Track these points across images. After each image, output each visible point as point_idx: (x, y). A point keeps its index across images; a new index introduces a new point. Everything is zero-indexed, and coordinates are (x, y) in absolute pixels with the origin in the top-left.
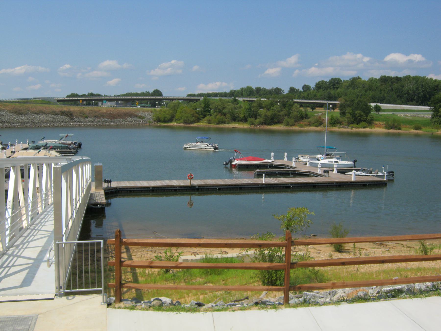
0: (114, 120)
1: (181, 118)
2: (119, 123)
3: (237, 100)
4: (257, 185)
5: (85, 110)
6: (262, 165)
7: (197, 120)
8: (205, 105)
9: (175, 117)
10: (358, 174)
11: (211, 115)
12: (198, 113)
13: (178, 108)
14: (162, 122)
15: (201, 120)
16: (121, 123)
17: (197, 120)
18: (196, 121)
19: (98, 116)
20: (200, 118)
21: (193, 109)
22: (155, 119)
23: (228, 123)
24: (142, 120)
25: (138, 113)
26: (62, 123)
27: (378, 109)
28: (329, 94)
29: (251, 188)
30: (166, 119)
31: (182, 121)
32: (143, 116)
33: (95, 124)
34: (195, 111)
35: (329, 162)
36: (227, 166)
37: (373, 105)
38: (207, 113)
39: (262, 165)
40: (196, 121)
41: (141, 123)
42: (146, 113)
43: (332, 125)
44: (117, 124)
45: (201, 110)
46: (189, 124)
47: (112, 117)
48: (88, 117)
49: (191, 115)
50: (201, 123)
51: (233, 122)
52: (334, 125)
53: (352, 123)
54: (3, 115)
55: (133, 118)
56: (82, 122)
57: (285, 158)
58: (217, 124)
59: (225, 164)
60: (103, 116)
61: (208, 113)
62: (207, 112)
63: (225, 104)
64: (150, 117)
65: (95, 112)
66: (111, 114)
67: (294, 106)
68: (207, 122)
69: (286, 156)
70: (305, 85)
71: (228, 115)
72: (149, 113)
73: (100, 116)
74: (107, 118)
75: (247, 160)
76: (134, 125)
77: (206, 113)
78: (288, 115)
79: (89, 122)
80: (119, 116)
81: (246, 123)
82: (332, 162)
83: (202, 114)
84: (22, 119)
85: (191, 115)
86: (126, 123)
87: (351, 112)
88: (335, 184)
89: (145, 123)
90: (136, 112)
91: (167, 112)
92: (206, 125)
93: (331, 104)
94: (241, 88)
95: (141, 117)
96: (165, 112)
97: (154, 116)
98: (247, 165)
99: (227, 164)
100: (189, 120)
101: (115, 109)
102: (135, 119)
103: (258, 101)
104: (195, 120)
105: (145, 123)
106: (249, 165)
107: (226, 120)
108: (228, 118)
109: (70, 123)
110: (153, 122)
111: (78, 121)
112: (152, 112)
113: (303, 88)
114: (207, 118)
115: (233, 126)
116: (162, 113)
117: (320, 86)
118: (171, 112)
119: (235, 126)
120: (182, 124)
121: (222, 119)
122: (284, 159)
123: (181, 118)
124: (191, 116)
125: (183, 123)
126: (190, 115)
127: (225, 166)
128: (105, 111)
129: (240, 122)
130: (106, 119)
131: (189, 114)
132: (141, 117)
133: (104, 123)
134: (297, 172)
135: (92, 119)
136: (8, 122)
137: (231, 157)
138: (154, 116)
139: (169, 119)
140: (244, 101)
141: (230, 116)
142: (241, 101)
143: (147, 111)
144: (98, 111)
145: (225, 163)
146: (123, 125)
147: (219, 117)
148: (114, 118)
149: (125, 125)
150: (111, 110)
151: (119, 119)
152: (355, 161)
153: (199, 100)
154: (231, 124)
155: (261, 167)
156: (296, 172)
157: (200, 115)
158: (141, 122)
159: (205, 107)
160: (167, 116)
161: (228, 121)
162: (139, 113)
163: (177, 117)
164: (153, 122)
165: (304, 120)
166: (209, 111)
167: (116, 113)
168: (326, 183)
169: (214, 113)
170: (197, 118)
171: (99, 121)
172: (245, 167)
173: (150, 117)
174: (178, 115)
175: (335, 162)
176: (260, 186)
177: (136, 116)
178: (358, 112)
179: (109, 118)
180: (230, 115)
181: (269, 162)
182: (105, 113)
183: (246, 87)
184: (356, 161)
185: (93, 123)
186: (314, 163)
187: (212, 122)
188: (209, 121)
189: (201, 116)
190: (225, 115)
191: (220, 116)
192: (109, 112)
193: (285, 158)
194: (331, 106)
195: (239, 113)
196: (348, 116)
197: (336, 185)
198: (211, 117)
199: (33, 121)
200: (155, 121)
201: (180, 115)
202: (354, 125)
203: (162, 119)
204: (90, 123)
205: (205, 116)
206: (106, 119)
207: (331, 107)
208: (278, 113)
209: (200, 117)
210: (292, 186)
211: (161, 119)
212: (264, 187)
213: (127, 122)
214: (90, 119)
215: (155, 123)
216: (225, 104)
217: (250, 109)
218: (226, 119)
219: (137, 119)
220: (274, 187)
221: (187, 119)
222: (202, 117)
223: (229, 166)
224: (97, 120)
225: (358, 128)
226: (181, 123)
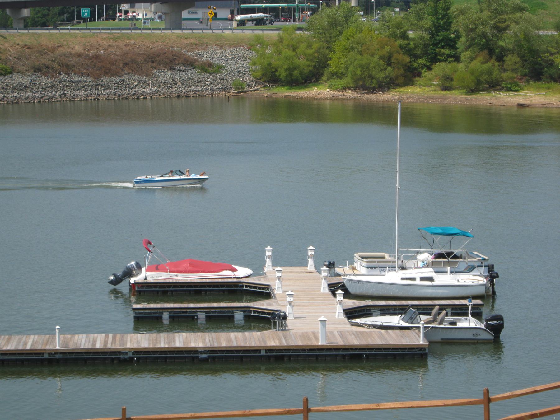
0: (106, 80)
1: (347, 68)
2: (125, 92)
4: (40, 354)
5: (6, 45)
6: (210, 286)
7: (404, 76)
8: (438, 19)
10: (380, 324)
11: (457, 59)
12: (409, 52)
14: (283, 86)
15: (419, 75)
16: (132, 92)
17: (404, 76)
18: (401, 80)
19: (48, 67)
20: (416, 69)
22: (259, 74)
23: (509, 90)
24: (209, 78)
25: (203, 52)
29: (22, 361)
30: (296, 73)
31: (347, 80)
32: (218, 61)
33: (34, 98)
34: (399, 42)
35: (403, 279)
36: (118, 287)
38: (443, 50)
39: (210, 286)
40: (401, 80)
41: (206, 90)
42: (229, 52)
44: (115, 94)
46: (372, 90)
47: (100, 68)
48: (11, 73)
49: (381, 58)
50: (418, 89)
51: (532, 83)
55: (180, 70)
57: (311, 262)
58: (473, 91)
59: (111, 282)
60: (68, 68)
61: (447, 52)
62: (442, 47)
63: (504, 16)
64: (242, 65)
65: (43, 51)
66: (97, 57)
68: (438, 85)
69: (312, 257)
71: (511, 60)
72: (242, 50)
73: (56, 65)
74: (82, 75)
75: (170, 272)
76: (178, 96)
77: (437, 50)
79: (15, 88)
80: (126, 64)
82: (413, 279)
83: (425, 54)
85: (381, 58)
86: (148, 90)
88: (263, 353)
89: (221, 89)
90: (193, 50)
92: (432, 94)
95: (207, 68)
96: (294, 50)
97: (254, 64)
98: (164, 287)
99: (117, 281)
100: (371, 77)
101: (115, 40)
102: (186, 76)
104: (397, 77)
105: (221, 89)
106: (169, 287)
107: (504, 75)
108: (514, 71)
110: (249, 85)
112: (251, 47)
114: (440, 68)
115: (522, 101)
116: (289, 53)
118: (315, 46)
119: (528, 102)
120: (350, 94)
121: (490, 72)
122: (306, 265)
123: (347, 68)
124: (382, 62)
125: (355, 89)
126: (376, 58)
127: (112, 287)
128: (78, 49)
129: (552, 84)
130: (76, 79)
131: (373, 55)
132: (210, 65)
133: (69, 93)
134: (254, 312)
135: (26, 80)
137: (131, 262)
138: (254, 64)
139: (306, 71)
141: (518, 60)
143: (236, 44)
144: (53, 50)
145: (112, 278)
146: (138, 98)
147: (479, 64)
148: (108, 72)
149: (145, 98)
150: (105, 43)
151: (126, 77)
152: (492, 275)
154: (522, 89)
155: (206, 291)
156: (250, 311)
157: (416, 57)
158: (205, 85)
159: (437, 28)
160: (302, 62)
161: (509, 81)
162: (203, 52)
163: (332, 68)
164: (249, 85)
166: (451, 44)
167: (118, 53)
168: (238, 351)
169: (467, 49)
170: (402, 71)
171: (52, 87)
172: (158, 291)
173: (242, 65)
176: (46, 356)
177: (191, 63)
179: (88, 75)
180: (522, 57)
181: (238, 278)
182: (79, 55)
184: (497, 276)
185: (29, 94)
186: (363, 282)
187: (454, 83)
188: (449, 78)
189: (422, 61)
190: (500, 59)
191: (483, 63)
192: (91, 53)
193: (311, 262)
195: (553, 51)
197: (269, 357)
200: (258, 80)
201: (342, 61)
203: (282, 74)
204: (16, 94)
206: (76, 79)
209: (416, 65)
210: (138, 359)
211: (277, 73)
212: (58, 360)
213: (153, 85)
214: (17, 79)
215: (259, 87)
216: (504, 16)
218: (505, 71)
219: (193, 74)
220: (85, 360)
221: (366, 73)
222: (425, 65)
223: (124, 287)
224: (45, 80)
226: (344, 89)
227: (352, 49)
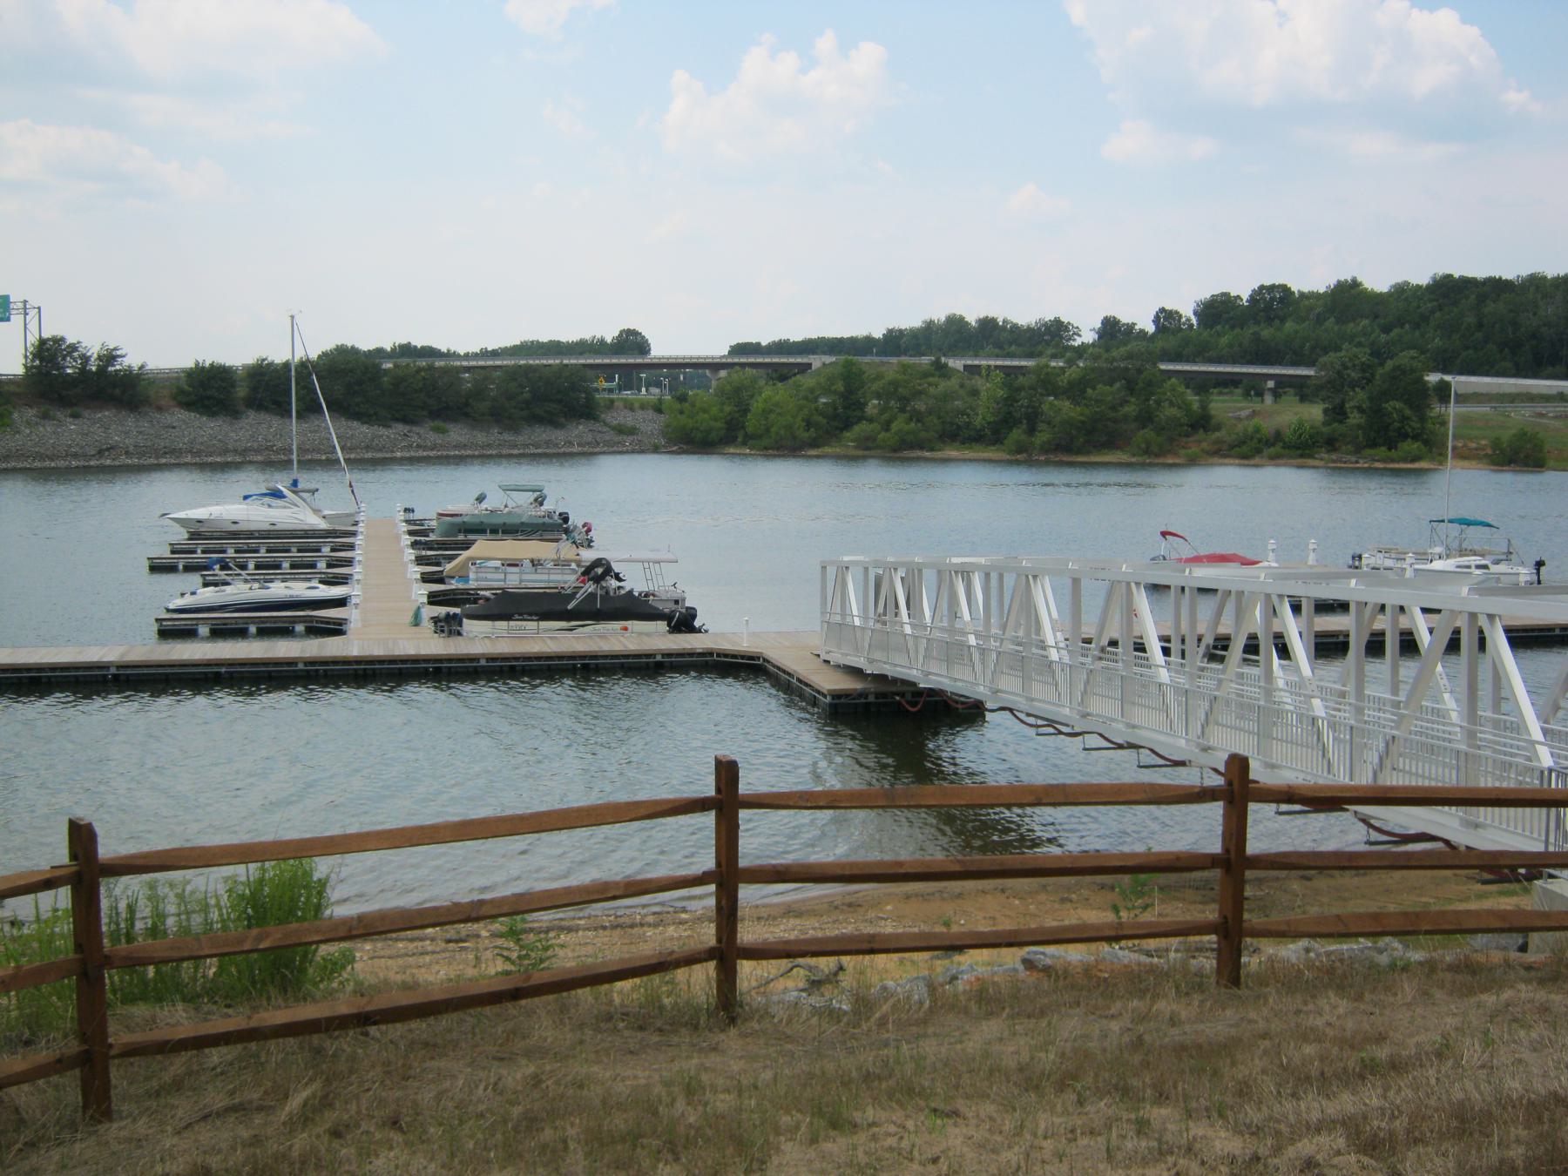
3: (946, 365)
9: (743, 427)
13: (752, 397)
21: (806, 398)
26: (367, 452)
27: (1443, 391)
28: (1257, 338)
37: (1433, 378)
43: (1300, 452)
45: (834, 401)
52: (1307, 452)
53: (1373, 444)
54: (174, 428)
56: (432, 450)
67: (1167, 385)
70: (1163, 310)
78: (1145, 419)
81: (997, 446)
82: (1469, 567)
84: (236, 441)
87: (1364, 406)
91: (714, 410)
93: (1270, 376)
94: (925, 322)
103: (1039, 369)
109: (393, 452)
111: (419, 446)
113: (1156, 320)
117: (1217, 310)
118: (728, 409)
136: (190, 452)
140: (965, 366)
142: (958, 371)
153: (809, 365)
165: (1201, 434)
166: (861, 406)
171: (488, 446)
174: (752, 423)
175: (1478, 567)
178: (1393, 405)
183: (943, 319)
194: (1271, 384)
196: (1355, 421)
198: (871, 426)
199: (272, 446)
202: (1382, 451)
205: (847, 425)
207: (1270, 389)
208: (1112, 414)
217: (1010, 400)
225: (1393, 461)
227: (771, 411)
